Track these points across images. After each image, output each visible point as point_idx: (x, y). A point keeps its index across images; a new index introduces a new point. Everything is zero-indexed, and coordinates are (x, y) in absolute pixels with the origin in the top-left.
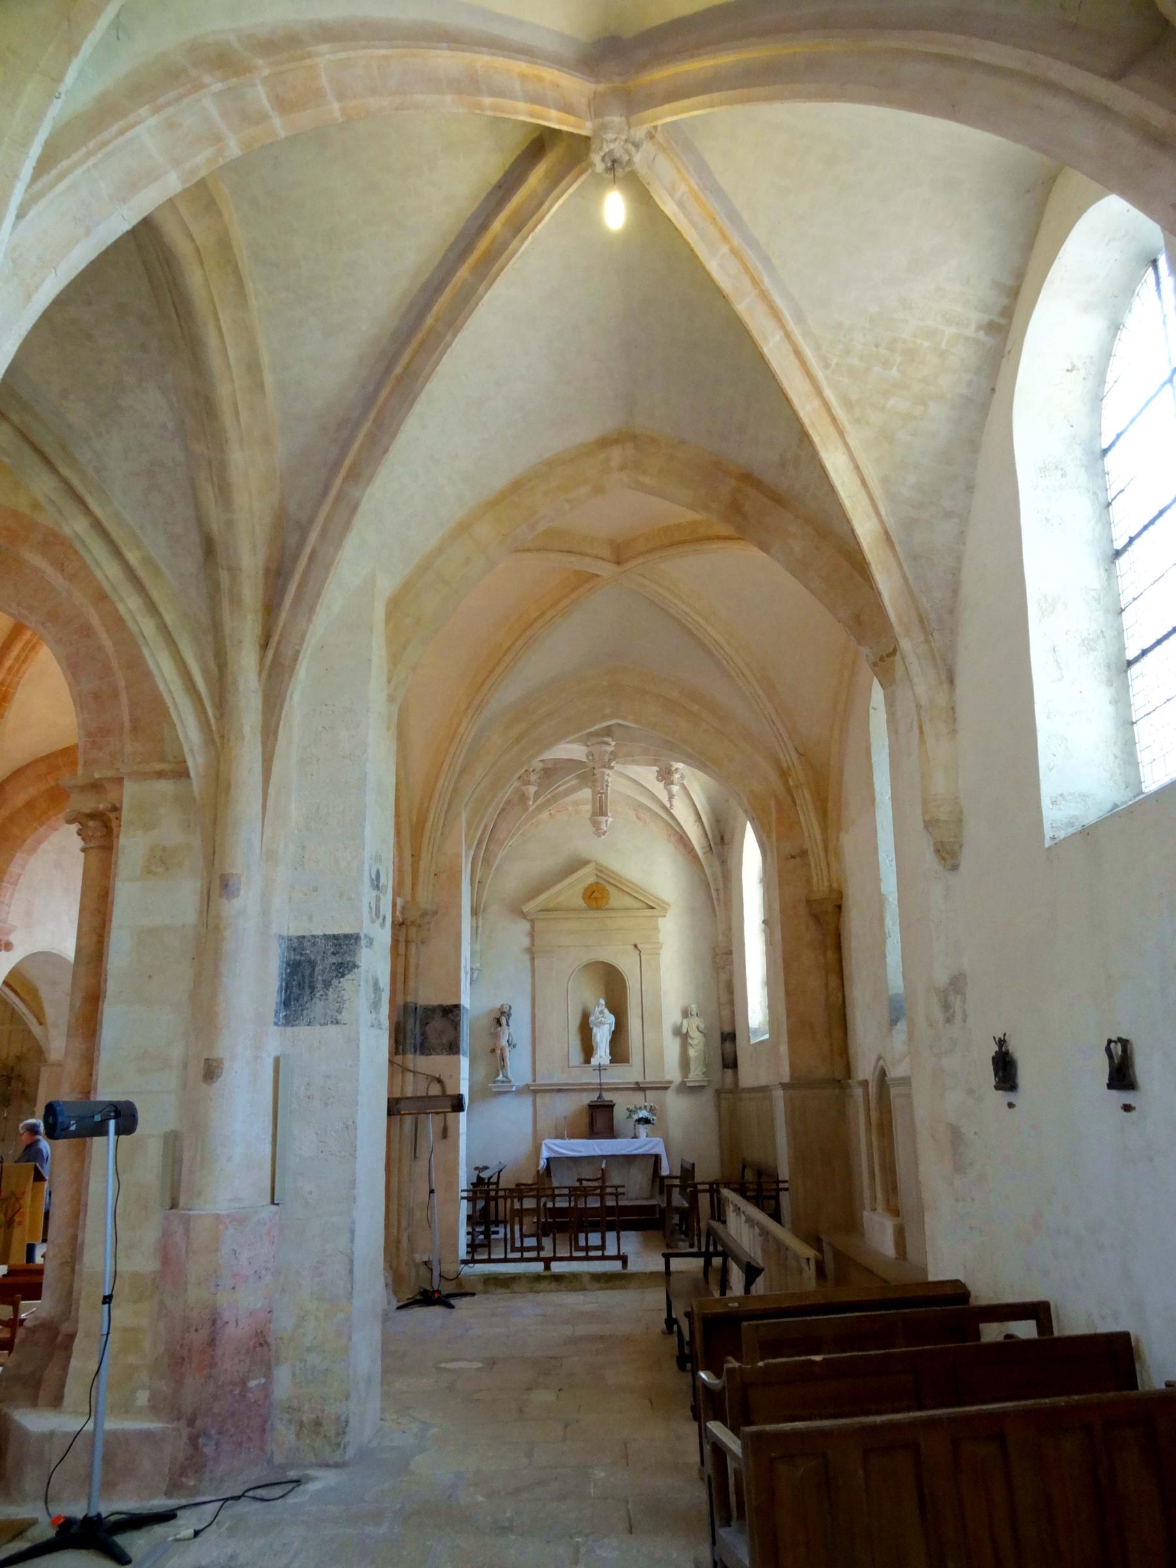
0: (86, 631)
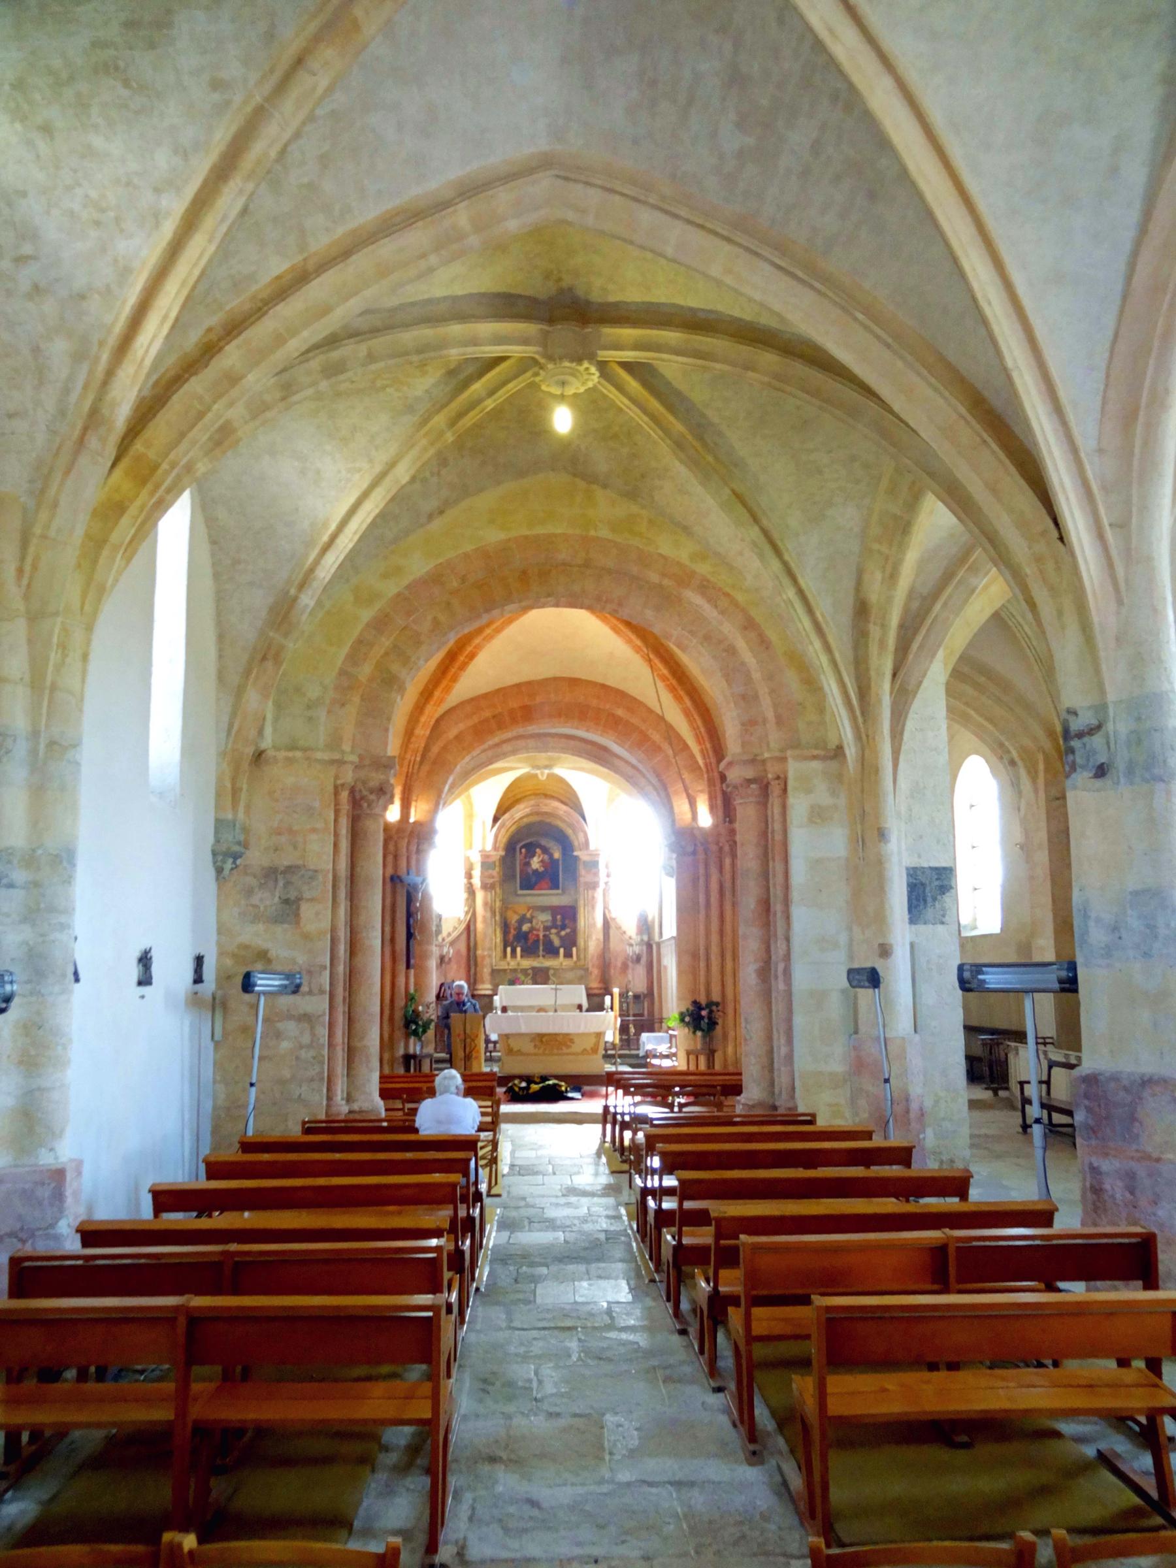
0: (731, 651)
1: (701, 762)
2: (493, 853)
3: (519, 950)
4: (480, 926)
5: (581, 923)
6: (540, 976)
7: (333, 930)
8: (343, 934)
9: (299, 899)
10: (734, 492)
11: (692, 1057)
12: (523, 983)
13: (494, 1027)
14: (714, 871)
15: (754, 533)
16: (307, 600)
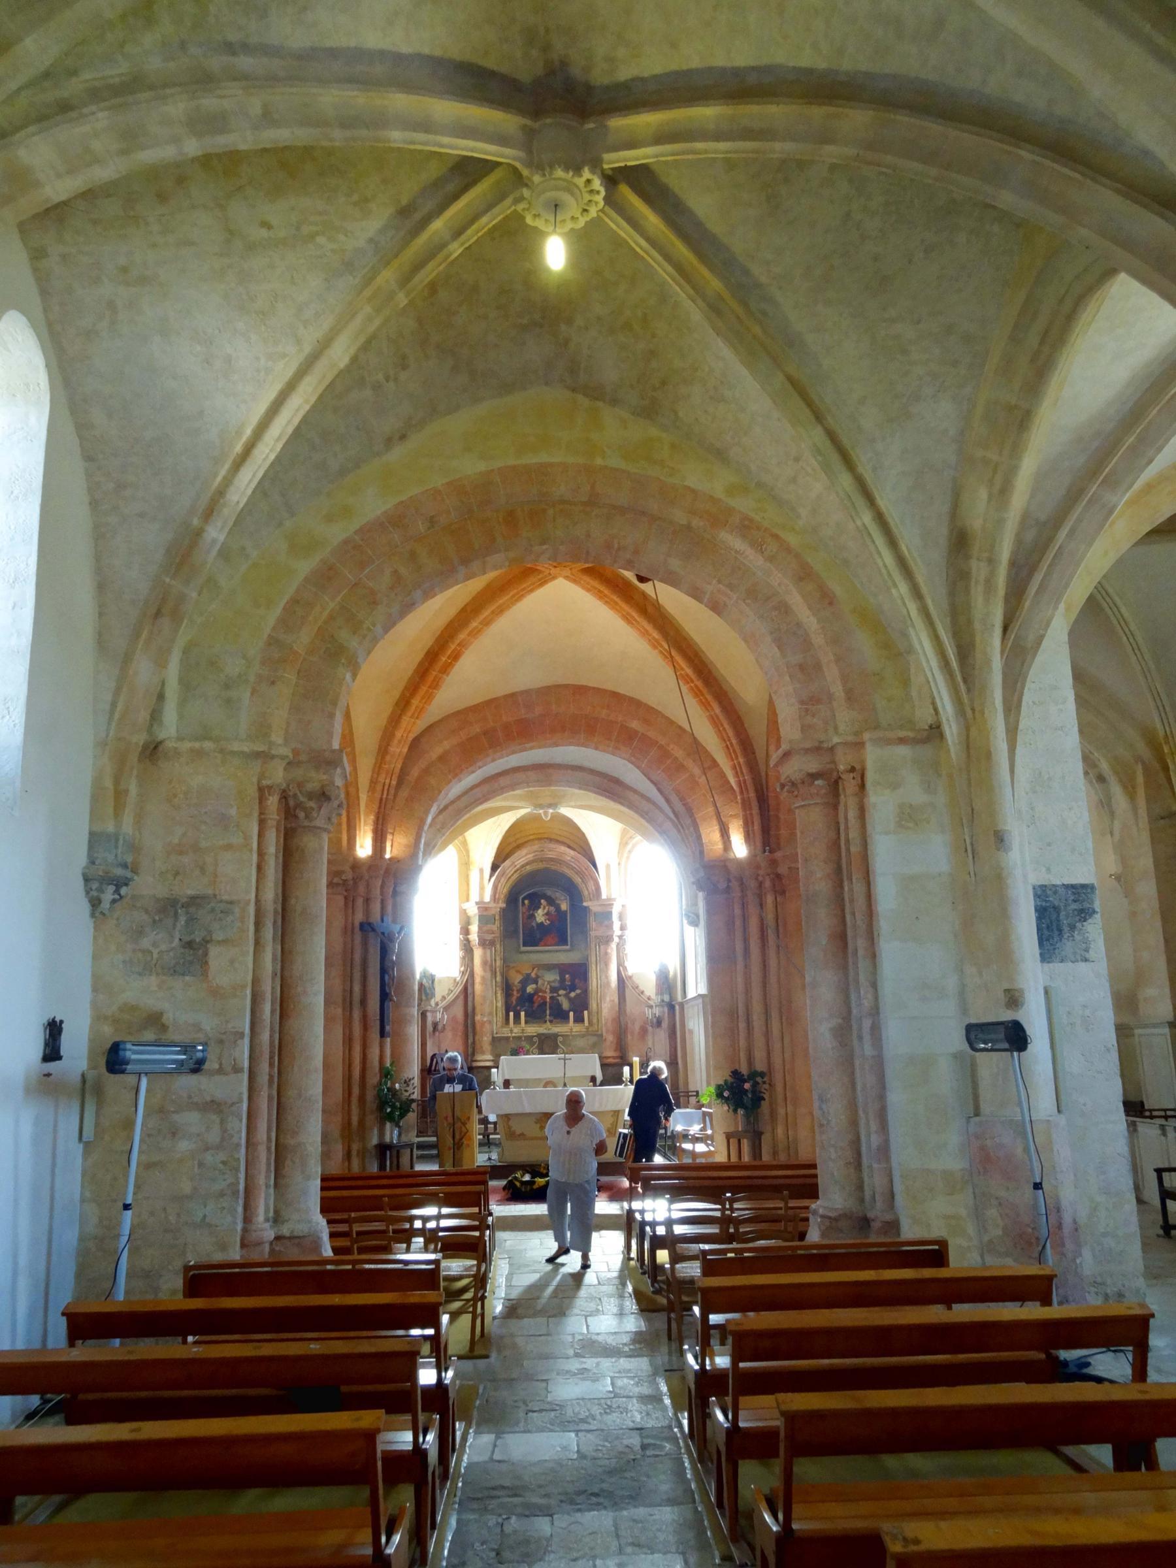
0: (784, 609)
1: (733, 781)
2: (492, 905)
3: (523, 1014)
4: (478, 987)
5: (593, 983)
6: (547, 1044)
7: (256, 981)
8: (269, 988)
9: (206, 942)
10: (790, 379)
11: (733, 1141)
12: (527, 1053)
13: (492, 1103)
14: (753, 910)
15: (818, 434)
16: (216, 533)
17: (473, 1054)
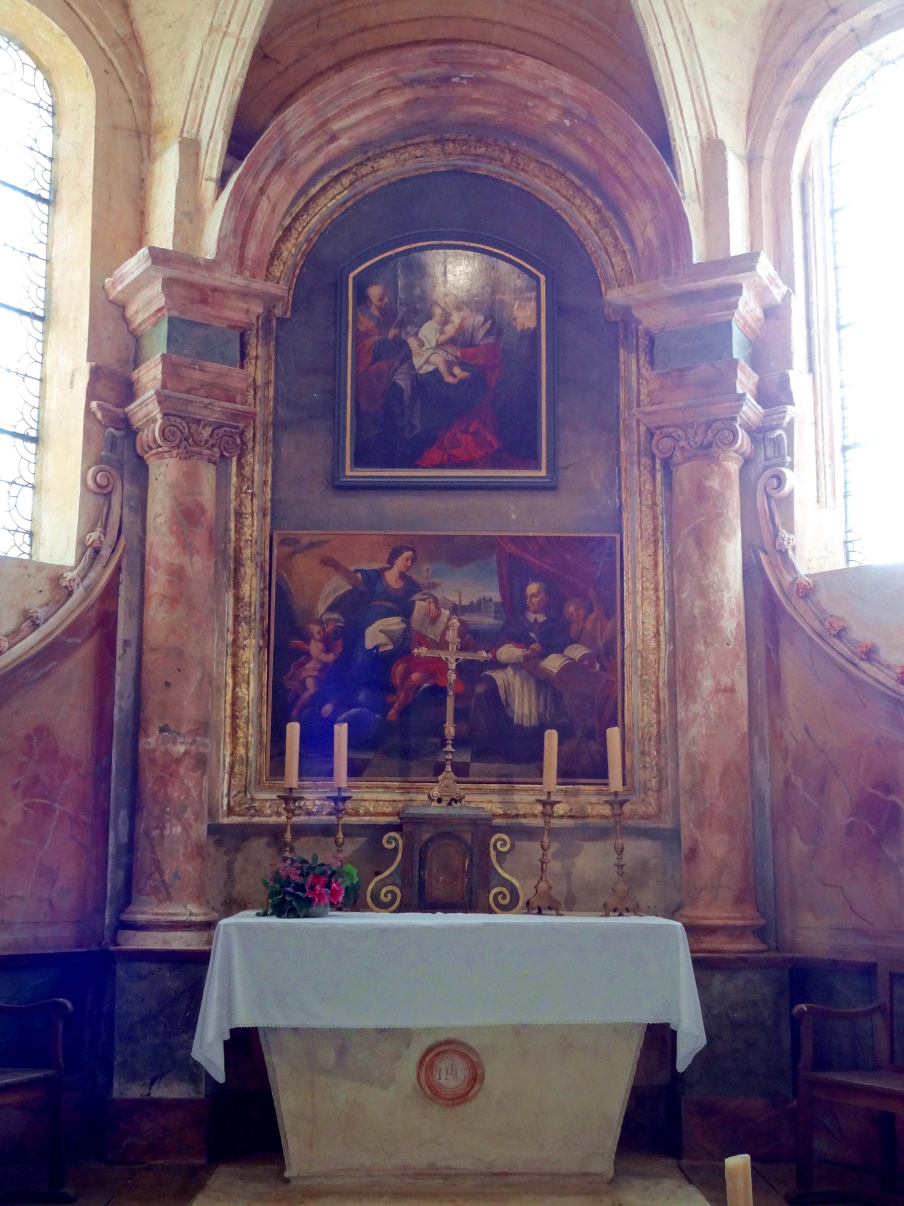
2: (226, 277)
3: (341, 732)
4: (157, 614)
5: (641, 617)
6: (443, 871)
12: (353, 901)
17: (127, 896)
